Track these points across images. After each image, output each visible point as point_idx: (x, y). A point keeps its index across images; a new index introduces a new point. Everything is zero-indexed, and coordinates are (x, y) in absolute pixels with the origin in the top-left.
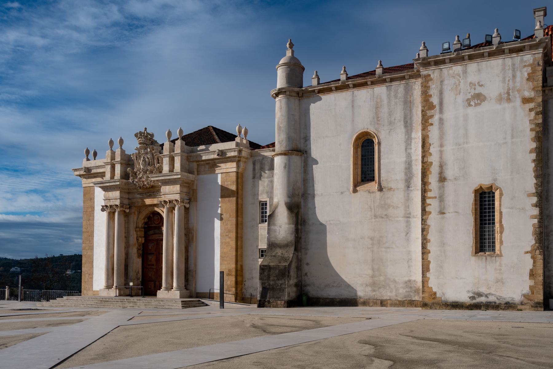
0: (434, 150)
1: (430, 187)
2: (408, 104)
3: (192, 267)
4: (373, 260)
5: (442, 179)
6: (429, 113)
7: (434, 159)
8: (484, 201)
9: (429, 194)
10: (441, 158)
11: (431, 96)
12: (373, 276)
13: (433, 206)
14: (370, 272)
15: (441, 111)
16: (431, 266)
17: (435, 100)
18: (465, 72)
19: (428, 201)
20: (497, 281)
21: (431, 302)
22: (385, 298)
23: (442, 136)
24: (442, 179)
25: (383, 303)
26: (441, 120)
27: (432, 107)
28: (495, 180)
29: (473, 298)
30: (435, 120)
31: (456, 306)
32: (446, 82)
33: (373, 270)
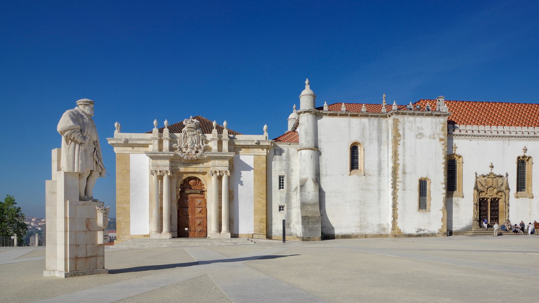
0: (400, 157)
1: (398, 176)
2: (380, 130)
4: (360, 213)
5: (404, 173)
6: (398, 138)
7: (400, 162)
8: (423, 185)
9: (398, 180)
10: (404, 162)
11: (399, 130)
12: (360, 222)
13: (400, 186)
14: (359, 220)
15: (404, 139)
18: (415, 121)
19: (397, 183)
20: (428, 223)
21: (398, 235)
22: (367, 233)
23: (404, 151)
24: (404, 173)
25: (366, 236)
27: (399, 135)
29: (418, 232)
30: (401, 142)
31: (410, 236)
32: (406, 124)
33: (360, 218)
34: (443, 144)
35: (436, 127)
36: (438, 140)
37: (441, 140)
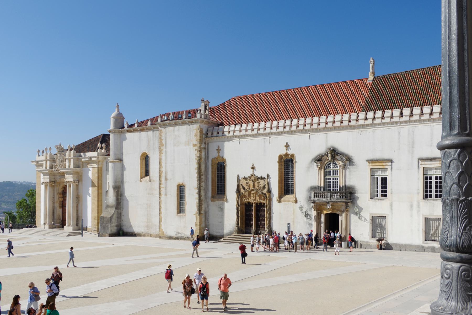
0: (163, 165)
3: (80, 215)
5: (166, 179)
6: (162, 148)
7: (163, 169)
10: (166, 169)
13: (163, 192)
15: (166, 148)
16: (163, 219)
17: (164, 142)
18: (174, 130)
24: (166, 179)
26: (166, 151)
27: (163, 145)
28: (184, 181)
29: (176, 234)
31: (171, 238)
32: (167, 134)
34: (196, 150)
35: (190, 134)
36: (192, 146)
37: (194, 145)
